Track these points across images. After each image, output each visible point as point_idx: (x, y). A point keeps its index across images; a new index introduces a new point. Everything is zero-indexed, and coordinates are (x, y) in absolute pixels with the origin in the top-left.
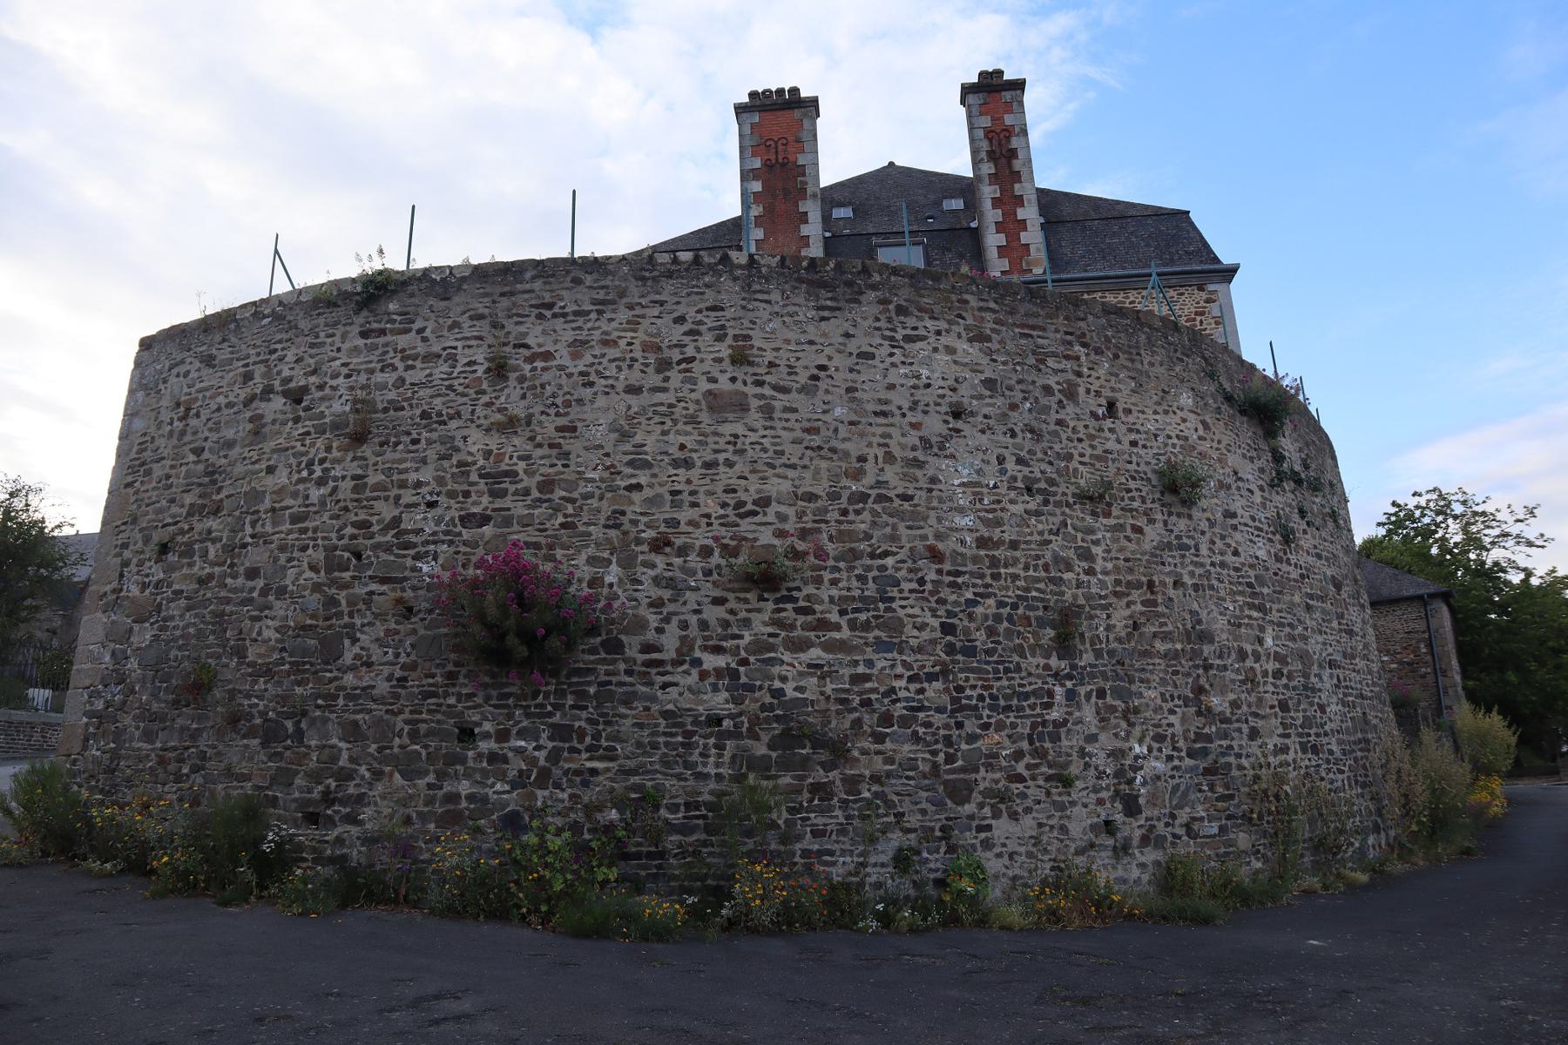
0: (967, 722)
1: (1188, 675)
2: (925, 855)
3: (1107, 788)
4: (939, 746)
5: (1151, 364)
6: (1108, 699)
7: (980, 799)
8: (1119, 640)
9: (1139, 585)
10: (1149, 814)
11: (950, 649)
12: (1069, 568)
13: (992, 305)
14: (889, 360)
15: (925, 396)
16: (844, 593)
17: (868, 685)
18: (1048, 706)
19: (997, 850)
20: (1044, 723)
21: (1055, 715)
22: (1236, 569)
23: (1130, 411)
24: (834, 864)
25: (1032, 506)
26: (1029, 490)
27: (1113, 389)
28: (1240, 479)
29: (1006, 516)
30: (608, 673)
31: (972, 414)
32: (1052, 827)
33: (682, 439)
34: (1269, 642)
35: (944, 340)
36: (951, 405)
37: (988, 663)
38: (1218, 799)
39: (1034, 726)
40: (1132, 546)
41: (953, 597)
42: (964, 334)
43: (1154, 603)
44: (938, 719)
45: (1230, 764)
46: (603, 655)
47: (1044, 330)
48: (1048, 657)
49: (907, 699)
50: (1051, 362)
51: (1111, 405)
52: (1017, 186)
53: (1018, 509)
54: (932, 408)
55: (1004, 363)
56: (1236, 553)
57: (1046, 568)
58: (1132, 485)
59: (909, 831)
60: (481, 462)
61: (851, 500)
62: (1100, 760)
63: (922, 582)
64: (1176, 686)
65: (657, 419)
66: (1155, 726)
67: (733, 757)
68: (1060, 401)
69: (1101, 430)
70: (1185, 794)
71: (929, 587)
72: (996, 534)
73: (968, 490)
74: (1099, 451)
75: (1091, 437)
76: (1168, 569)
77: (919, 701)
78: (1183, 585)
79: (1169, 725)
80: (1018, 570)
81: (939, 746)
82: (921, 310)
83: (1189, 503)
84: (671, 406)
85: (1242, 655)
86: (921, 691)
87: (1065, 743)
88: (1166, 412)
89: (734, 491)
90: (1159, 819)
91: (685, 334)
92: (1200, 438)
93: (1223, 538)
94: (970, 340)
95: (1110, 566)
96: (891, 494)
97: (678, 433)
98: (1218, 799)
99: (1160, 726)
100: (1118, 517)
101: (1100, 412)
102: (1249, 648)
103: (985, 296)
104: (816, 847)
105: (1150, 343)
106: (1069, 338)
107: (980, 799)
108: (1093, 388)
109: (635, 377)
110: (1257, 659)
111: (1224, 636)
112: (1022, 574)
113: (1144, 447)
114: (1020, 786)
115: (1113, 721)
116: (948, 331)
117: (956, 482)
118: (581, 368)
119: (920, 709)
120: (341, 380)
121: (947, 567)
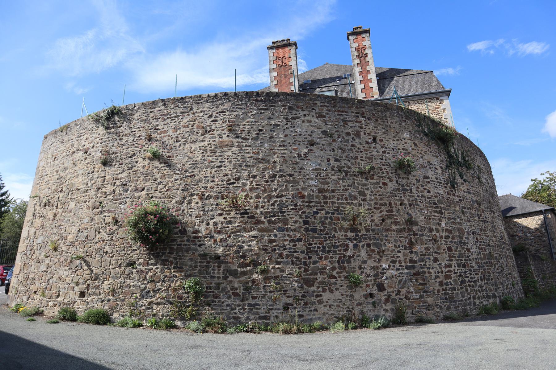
0: (313, 257)
1: (407, 238)
2: (295, 306)
3: (371, 281)
4: (302, 266)
5: (392, 123)
6: (372, 247)
7: (318, 285)
8: (377, 225)
9: (385, 204)
10: (389, 290)
11: (307, 230)
12: (356, 198)
13: (326, 104)
14: (286, 126)
15: (299, 139)
16: (266, 210)
17: (274, 244)
18: (346, 250)
19: (324, 304)
20: (344, 257)
21: (349, 253)
22: (429, 198)
23: (382, 140)
24: (260, 309)
25: (341, 176)
26: (340, 171)
27: (375, 133)
28: (431, 164)
29: (330, 181)
30: (181, 241)
31: (317, 144)
32: (347, 295)
33: (210, 158)
34: (443, 225)
35: (307, 118)
36: (309, 141)
37: (322, 235)
38: (420, 285)
39: (340, 258)
40: (383, 190)
41: (309, 211)
42: (315, 115)
43: (392, 211)
44: (302, 256)
45: (425, 272)
46: (180, 235)
47: (347, 112)
48: (346, 232)
49: (290, 248)
50: (350, 124)
51: (374, 139)
52: (368, 67)
53: (335, 178)
54: (301, 143)
55: (331, 125)
56: (429, 192)
57: (346, 199)
58: (383, 167)
59: (288, 297)
60: (142, 170)
61: (270, 177)
62: (368, 270)
63: (296, 205)
64: (401, 242)
65: (201, 152)
66: (391, 257)
67: (224, 270)
68: (353, 138)
69: (370, 147)
70: (405, 283)
71: (299, 207)
72: (326, 187)
73: (315, 172)
74: (369, 155)
75: (366, 150)
76: (398, 198)
77: (294, 249)
78: (405, 204)
79: (397, 257)
80: (335, 200)
81: (302, 266)
82: (298, 108)
83: (409, 173)
84: (206, 147)
85: (431, 230)
86: (295, 245)
87: (353, 264)
88: (398, 140)
89: (227, 175)
90: (393, 292)
91: (212, 121)
92: (413, 149)
93: (423, 186)
94: (317, 118)
95: (373, 198)
96: (285, 174)
97: (208, 156)
98: (420, 285)
99: (394, 257)
100: (376, 180)
101: (370, 141)
102: (434, 227)
103: (324, 101)
104: (253, 303)
105: (391, 115)
106: (357, 115)
107: (318, 285)
108: (367, 132)
109: (194, 137)
110: (438, 231)
111: (423, 223)
112: (336, 201)
113: (388, 153)
114: (334, 280)
115: (373, 255)
116: (308, 115)
117: (310, 169)
118: (176, 135)
119: (294, 252)
120: (99, 144)
121: (306, 200)
